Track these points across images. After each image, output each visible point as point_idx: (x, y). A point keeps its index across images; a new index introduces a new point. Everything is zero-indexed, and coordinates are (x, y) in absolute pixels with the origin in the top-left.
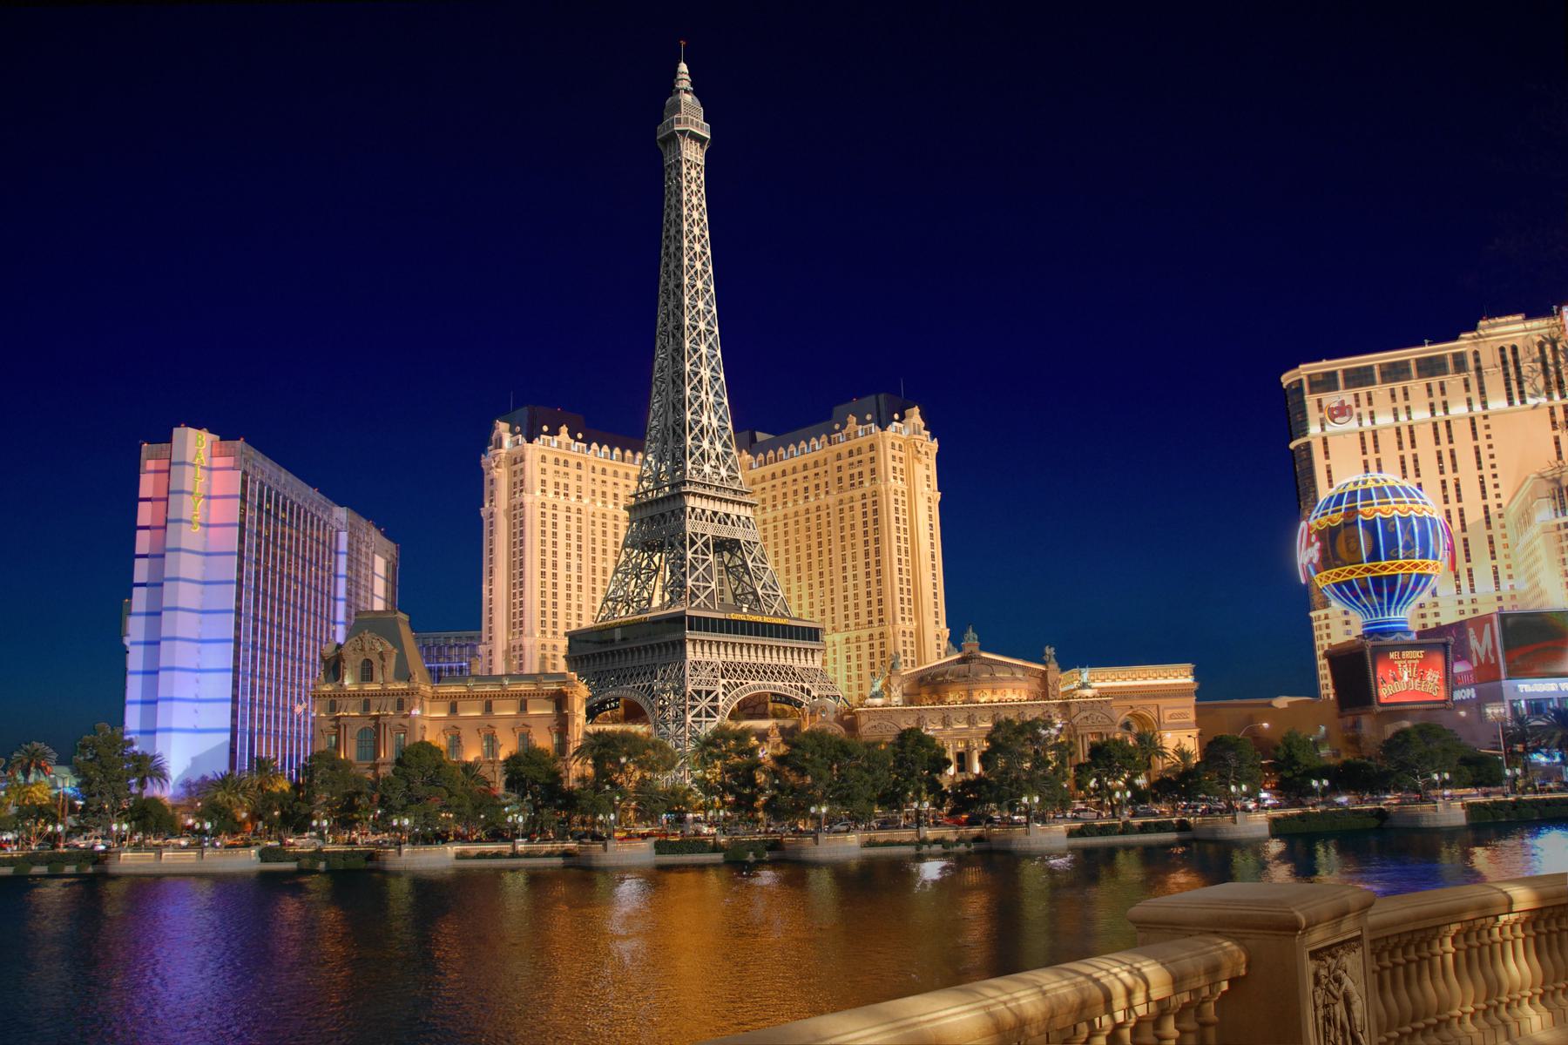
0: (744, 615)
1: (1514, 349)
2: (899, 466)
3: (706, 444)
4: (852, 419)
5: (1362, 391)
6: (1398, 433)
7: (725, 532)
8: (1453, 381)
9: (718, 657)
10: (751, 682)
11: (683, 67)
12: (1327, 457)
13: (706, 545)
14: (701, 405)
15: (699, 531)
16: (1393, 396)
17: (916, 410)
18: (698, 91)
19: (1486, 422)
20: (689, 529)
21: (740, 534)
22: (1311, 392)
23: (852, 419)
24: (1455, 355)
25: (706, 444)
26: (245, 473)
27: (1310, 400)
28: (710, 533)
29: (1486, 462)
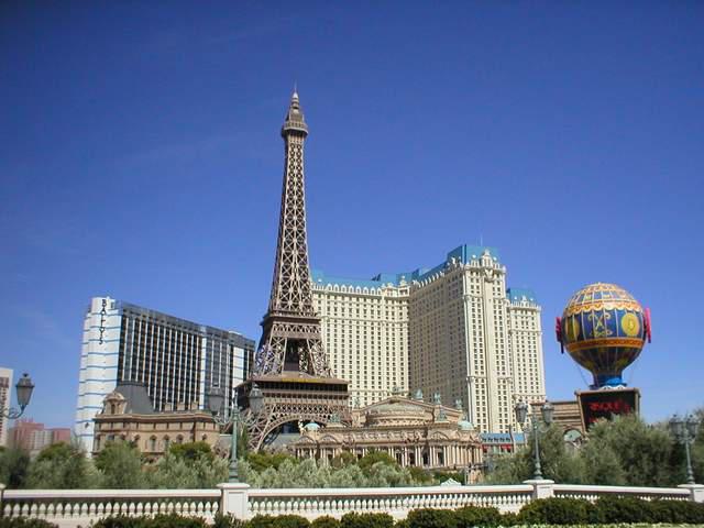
0: (302, 377)
3: (291, 290)
7: (296, 336)
9: (274, 401)
10: (292, 414)
11: (296, 96)
13: (283, 343)
14: (290, 271)
15: (279, 335)
18: (305, 106)
20: (272, 335)
21: (307, 336)
25: (291, 290)
26: (124, 316)
28: (287, 335)
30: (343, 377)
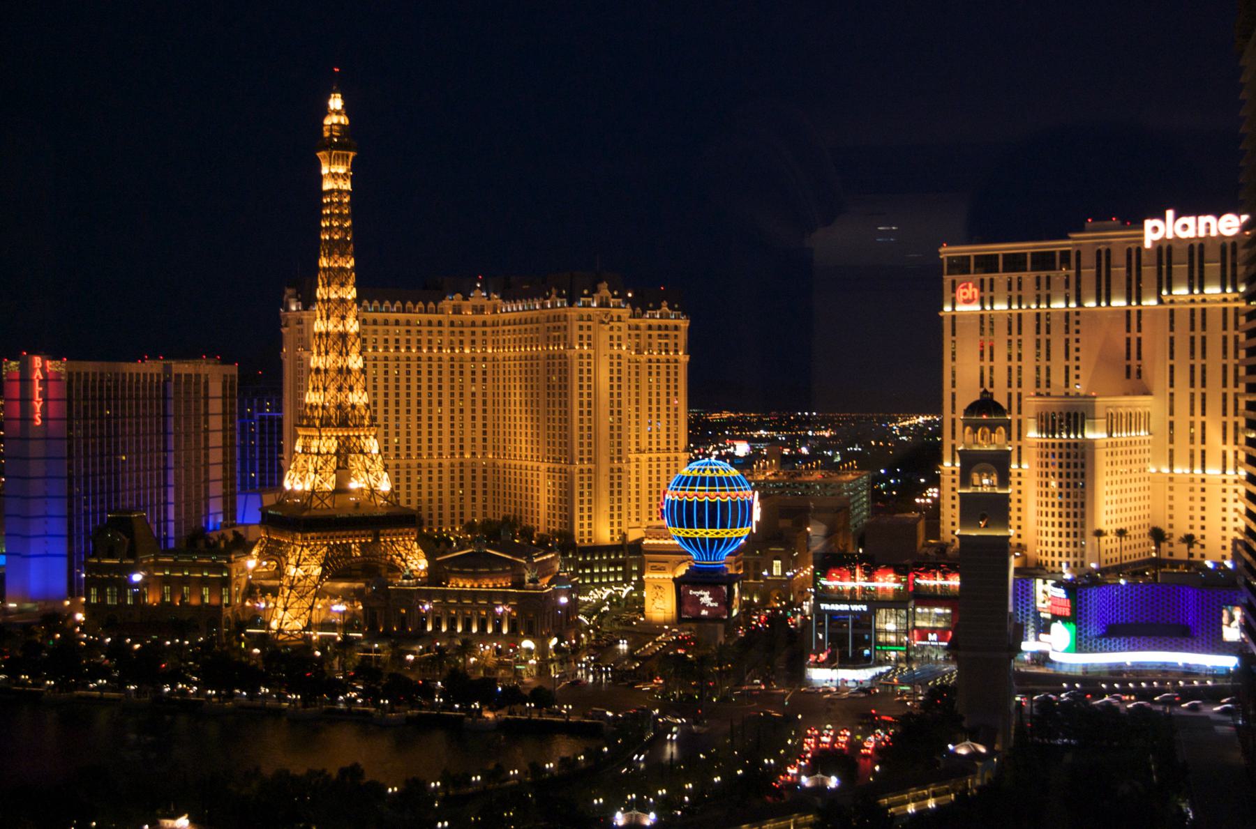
1: (1108, 251)
2: (585, 333)
4: (554, 290)
5: (987, 277)
6: (1010, 323)
8: (1059, 275)
12: (954, 334)
16: (1010, 284)
17: (605, 285)
19: (1078, 318)
22: (949, 274)
23: (554, 290)
24: (1062, 252)
27: (947, 280)
29: (1073, 354)
30: (409, 502)
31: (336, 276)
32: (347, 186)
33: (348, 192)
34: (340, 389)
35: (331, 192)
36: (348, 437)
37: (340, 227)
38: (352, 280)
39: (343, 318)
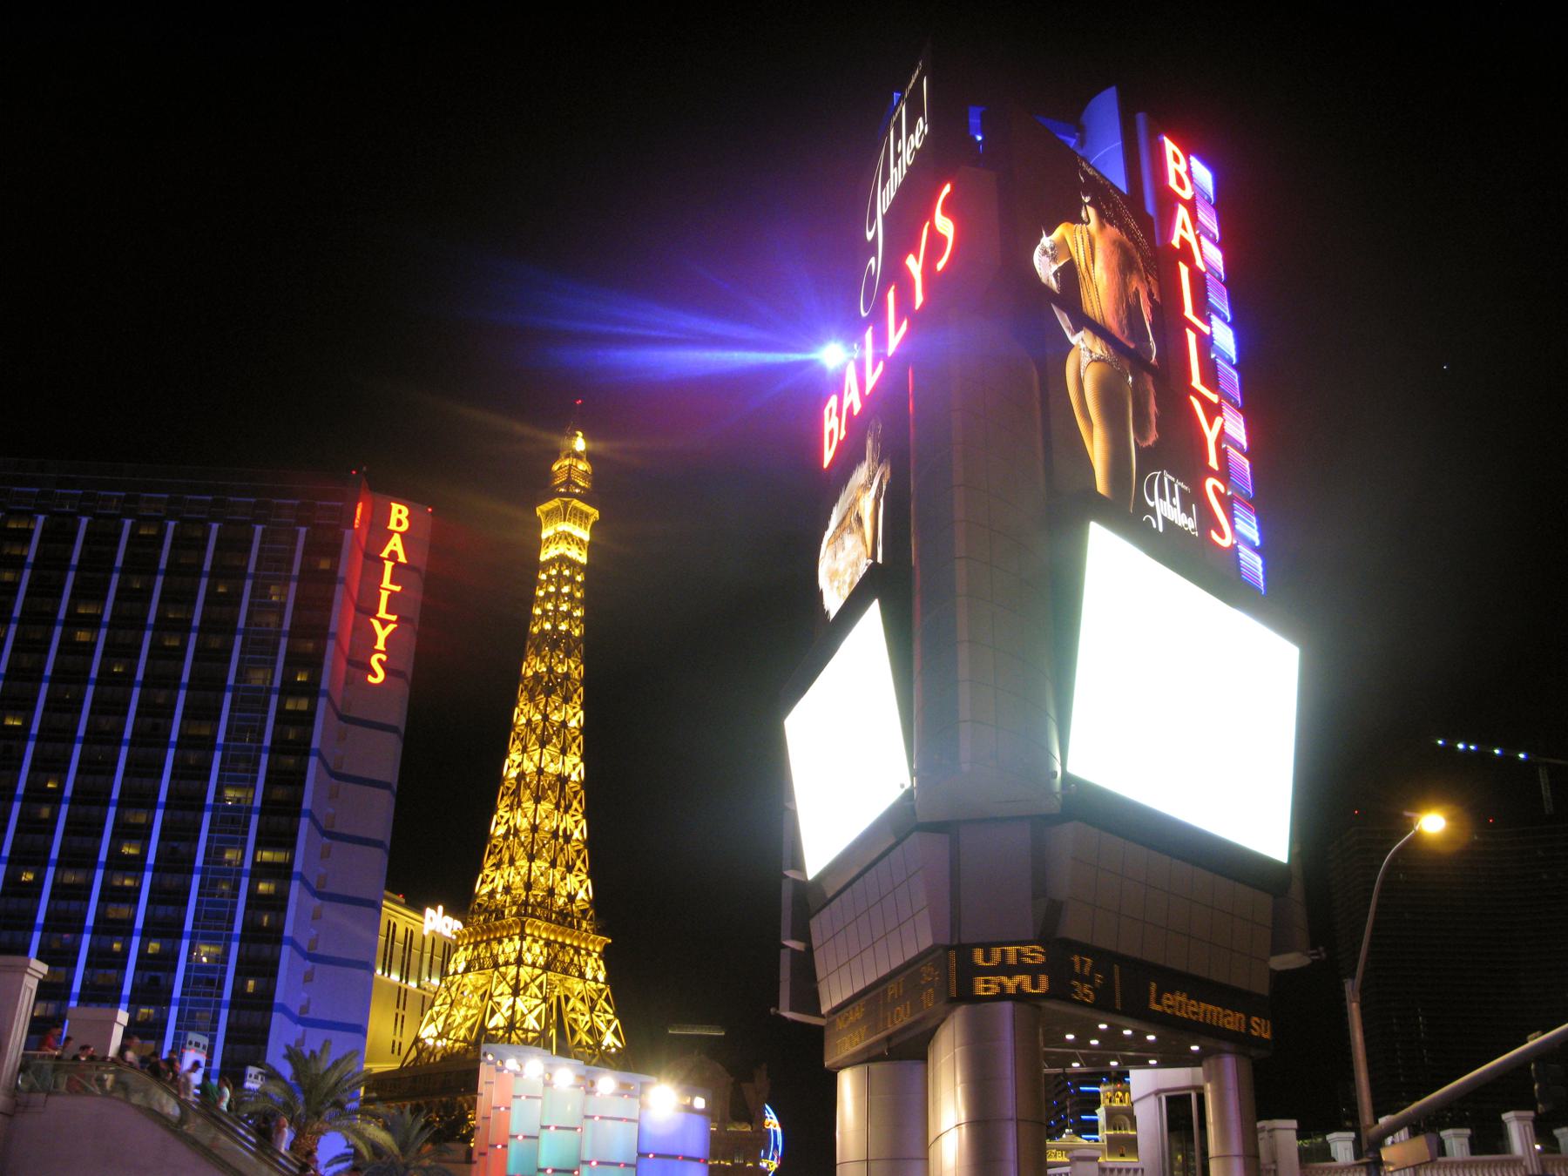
31: (549, 686)
32: (583, 558)
33: (582, 566)
34: (553, 864)
35: (562, 560)
36: (563, 945)
37: (568, 615)
38: (577, 700)
39: (564, 752)
